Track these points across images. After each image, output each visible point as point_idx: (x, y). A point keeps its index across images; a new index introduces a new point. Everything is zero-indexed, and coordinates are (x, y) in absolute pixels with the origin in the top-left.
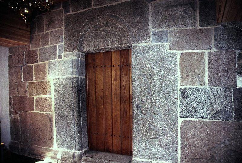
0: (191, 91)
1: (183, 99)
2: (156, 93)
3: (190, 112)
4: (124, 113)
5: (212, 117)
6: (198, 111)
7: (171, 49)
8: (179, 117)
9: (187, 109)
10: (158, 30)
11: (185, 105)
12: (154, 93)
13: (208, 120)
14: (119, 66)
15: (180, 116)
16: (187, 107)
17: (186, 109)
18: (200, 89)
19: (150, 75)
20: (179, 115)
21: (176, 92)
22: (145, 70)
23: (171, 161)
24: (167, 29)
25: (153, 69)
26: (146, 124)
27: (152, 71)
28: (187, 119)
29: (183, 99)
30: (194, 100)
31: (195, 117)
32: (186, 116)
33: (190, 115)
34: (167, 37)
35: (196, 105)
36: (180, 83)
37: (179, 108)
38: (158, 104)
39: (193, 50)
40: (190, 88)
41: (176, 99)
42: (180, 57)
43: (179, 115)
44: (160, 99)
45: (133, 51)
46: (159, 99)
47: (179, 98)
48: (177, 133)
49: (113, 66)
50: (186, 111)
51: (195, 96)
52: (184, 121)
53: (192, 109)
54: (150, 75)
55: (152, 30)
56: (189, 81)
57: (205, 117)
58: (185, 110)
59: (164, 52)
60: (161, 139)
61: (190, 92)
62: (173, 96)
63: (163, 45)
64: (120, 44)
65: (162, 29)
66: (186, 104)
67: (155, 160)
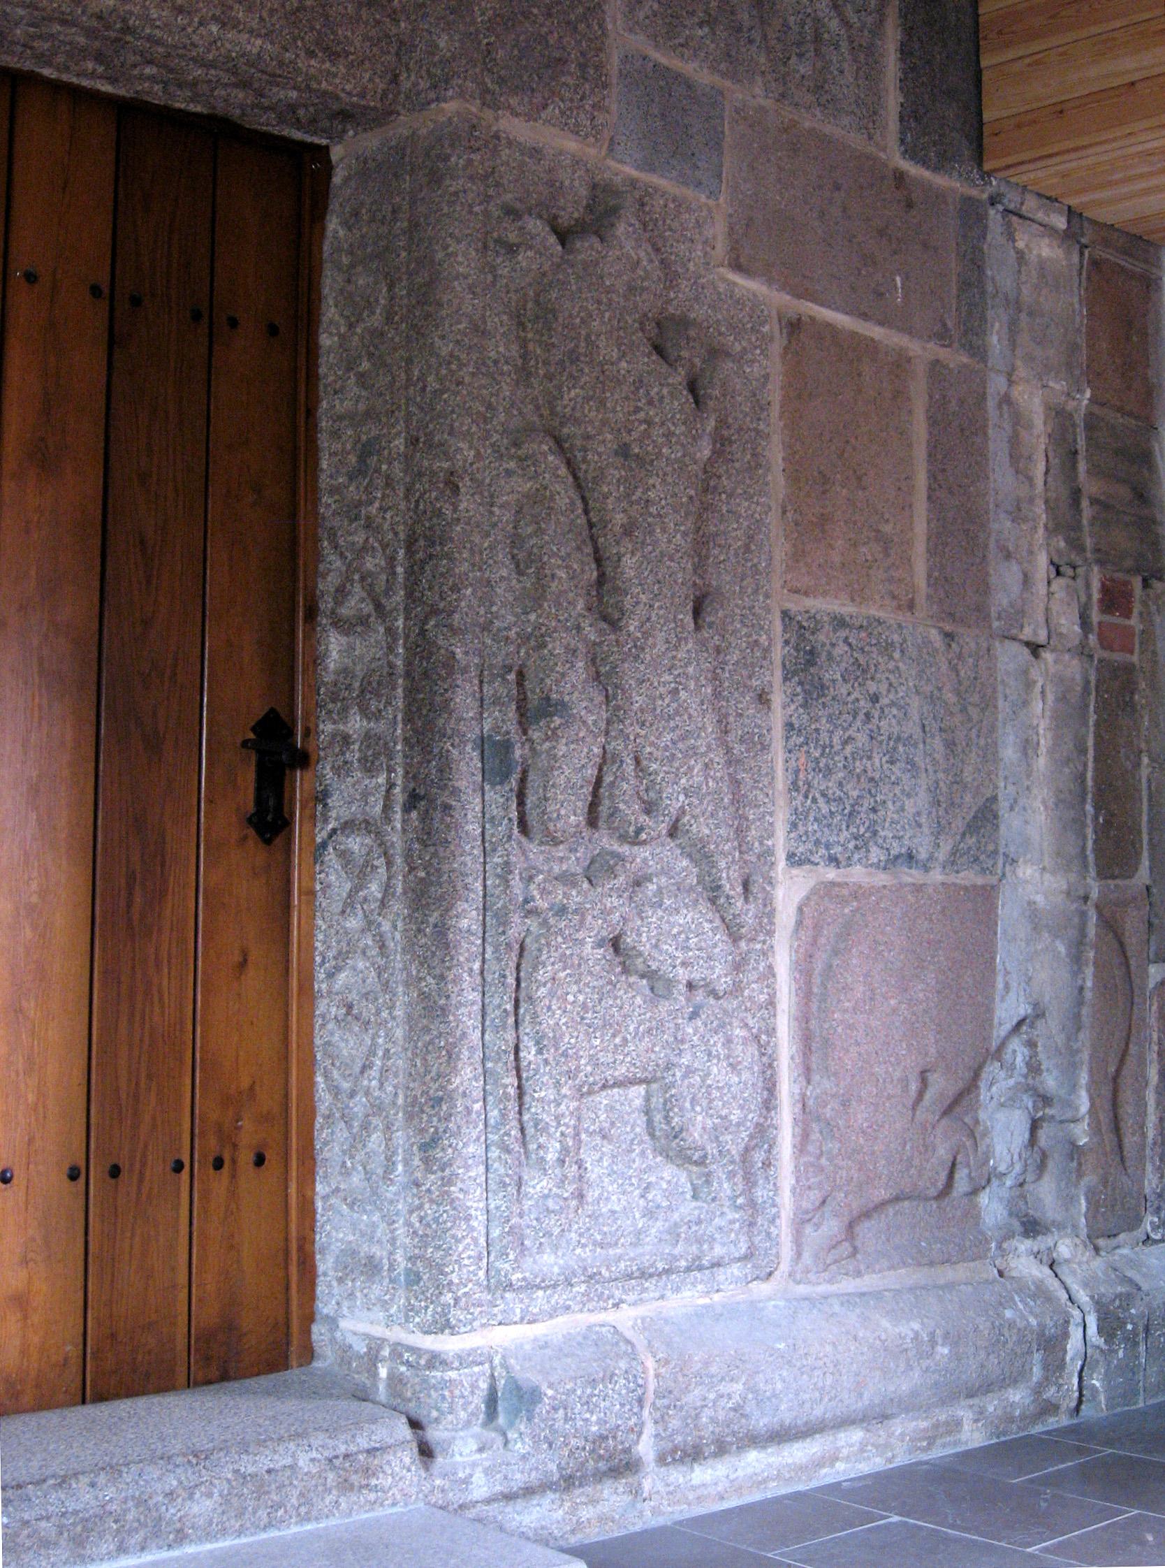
0: (846, 640)
1: (805, 705)
2: (661, 636)
3: (851, 814)
4: (131, 877)
5: (954, 852)
6: (890, 804)
7: (737, 267)
8: (782, 864)
9: (834, 791)
10: (664, 61)
11: (817, 761)
12: (646, 635)
13: (937, 876)
14: (95, 291)
15: (791, 856)
16: (828, 772)
17: (824, 795)
18: (896, 637)
19: (624, 451)
20: (780, 842)
21: (763, 639)
22: (587, 399)
23: (735, 1270)
24: (717, 80)
25: (650, 403)
26: (582, 942)
27: (641, 415)
28: (831, 874)
29: (805, 705)
30: (868, 716)
31: (876, 854)
32: (828, 847)
33: (851, 846)
34: (718, 146)
35: (877, 764)
36: (789, 569)
37: (781, 782)
38: (667, 737)
39: (865, 316)
40: (840, 622)
41: (763, 699)
42: (786, 349)
43: (780, 842)
44: (683, 695)
45: (471, 178)
46: (675, 692)
47: (777, 699)
48: (771, 1003)
49: (31, 278)
50: (825, 809)
51: (872, 687)
52: (814, 891)
53: (855, 793)
54: (624, 451)
55: (625, 39)
56: (837, 559)
57: (923, 855)
58: (821, 800)
59: (691, 266)
60: (689, 1072)
61: (841, 649)
62: (745, 673)
63: (689, 210)
64: (311, 54)
65: (689, 68)
66: (824, 747)
67: (632, 1297)
